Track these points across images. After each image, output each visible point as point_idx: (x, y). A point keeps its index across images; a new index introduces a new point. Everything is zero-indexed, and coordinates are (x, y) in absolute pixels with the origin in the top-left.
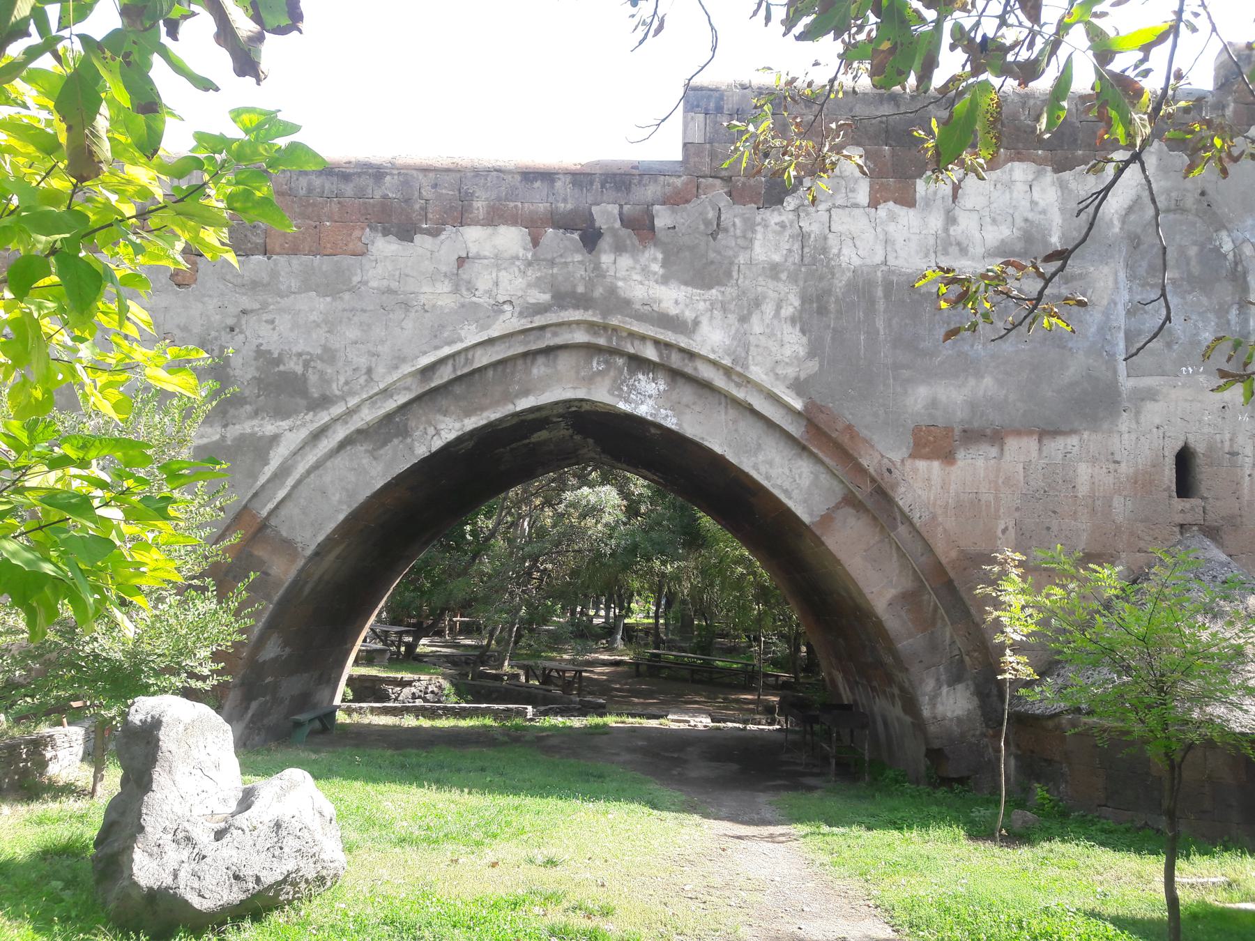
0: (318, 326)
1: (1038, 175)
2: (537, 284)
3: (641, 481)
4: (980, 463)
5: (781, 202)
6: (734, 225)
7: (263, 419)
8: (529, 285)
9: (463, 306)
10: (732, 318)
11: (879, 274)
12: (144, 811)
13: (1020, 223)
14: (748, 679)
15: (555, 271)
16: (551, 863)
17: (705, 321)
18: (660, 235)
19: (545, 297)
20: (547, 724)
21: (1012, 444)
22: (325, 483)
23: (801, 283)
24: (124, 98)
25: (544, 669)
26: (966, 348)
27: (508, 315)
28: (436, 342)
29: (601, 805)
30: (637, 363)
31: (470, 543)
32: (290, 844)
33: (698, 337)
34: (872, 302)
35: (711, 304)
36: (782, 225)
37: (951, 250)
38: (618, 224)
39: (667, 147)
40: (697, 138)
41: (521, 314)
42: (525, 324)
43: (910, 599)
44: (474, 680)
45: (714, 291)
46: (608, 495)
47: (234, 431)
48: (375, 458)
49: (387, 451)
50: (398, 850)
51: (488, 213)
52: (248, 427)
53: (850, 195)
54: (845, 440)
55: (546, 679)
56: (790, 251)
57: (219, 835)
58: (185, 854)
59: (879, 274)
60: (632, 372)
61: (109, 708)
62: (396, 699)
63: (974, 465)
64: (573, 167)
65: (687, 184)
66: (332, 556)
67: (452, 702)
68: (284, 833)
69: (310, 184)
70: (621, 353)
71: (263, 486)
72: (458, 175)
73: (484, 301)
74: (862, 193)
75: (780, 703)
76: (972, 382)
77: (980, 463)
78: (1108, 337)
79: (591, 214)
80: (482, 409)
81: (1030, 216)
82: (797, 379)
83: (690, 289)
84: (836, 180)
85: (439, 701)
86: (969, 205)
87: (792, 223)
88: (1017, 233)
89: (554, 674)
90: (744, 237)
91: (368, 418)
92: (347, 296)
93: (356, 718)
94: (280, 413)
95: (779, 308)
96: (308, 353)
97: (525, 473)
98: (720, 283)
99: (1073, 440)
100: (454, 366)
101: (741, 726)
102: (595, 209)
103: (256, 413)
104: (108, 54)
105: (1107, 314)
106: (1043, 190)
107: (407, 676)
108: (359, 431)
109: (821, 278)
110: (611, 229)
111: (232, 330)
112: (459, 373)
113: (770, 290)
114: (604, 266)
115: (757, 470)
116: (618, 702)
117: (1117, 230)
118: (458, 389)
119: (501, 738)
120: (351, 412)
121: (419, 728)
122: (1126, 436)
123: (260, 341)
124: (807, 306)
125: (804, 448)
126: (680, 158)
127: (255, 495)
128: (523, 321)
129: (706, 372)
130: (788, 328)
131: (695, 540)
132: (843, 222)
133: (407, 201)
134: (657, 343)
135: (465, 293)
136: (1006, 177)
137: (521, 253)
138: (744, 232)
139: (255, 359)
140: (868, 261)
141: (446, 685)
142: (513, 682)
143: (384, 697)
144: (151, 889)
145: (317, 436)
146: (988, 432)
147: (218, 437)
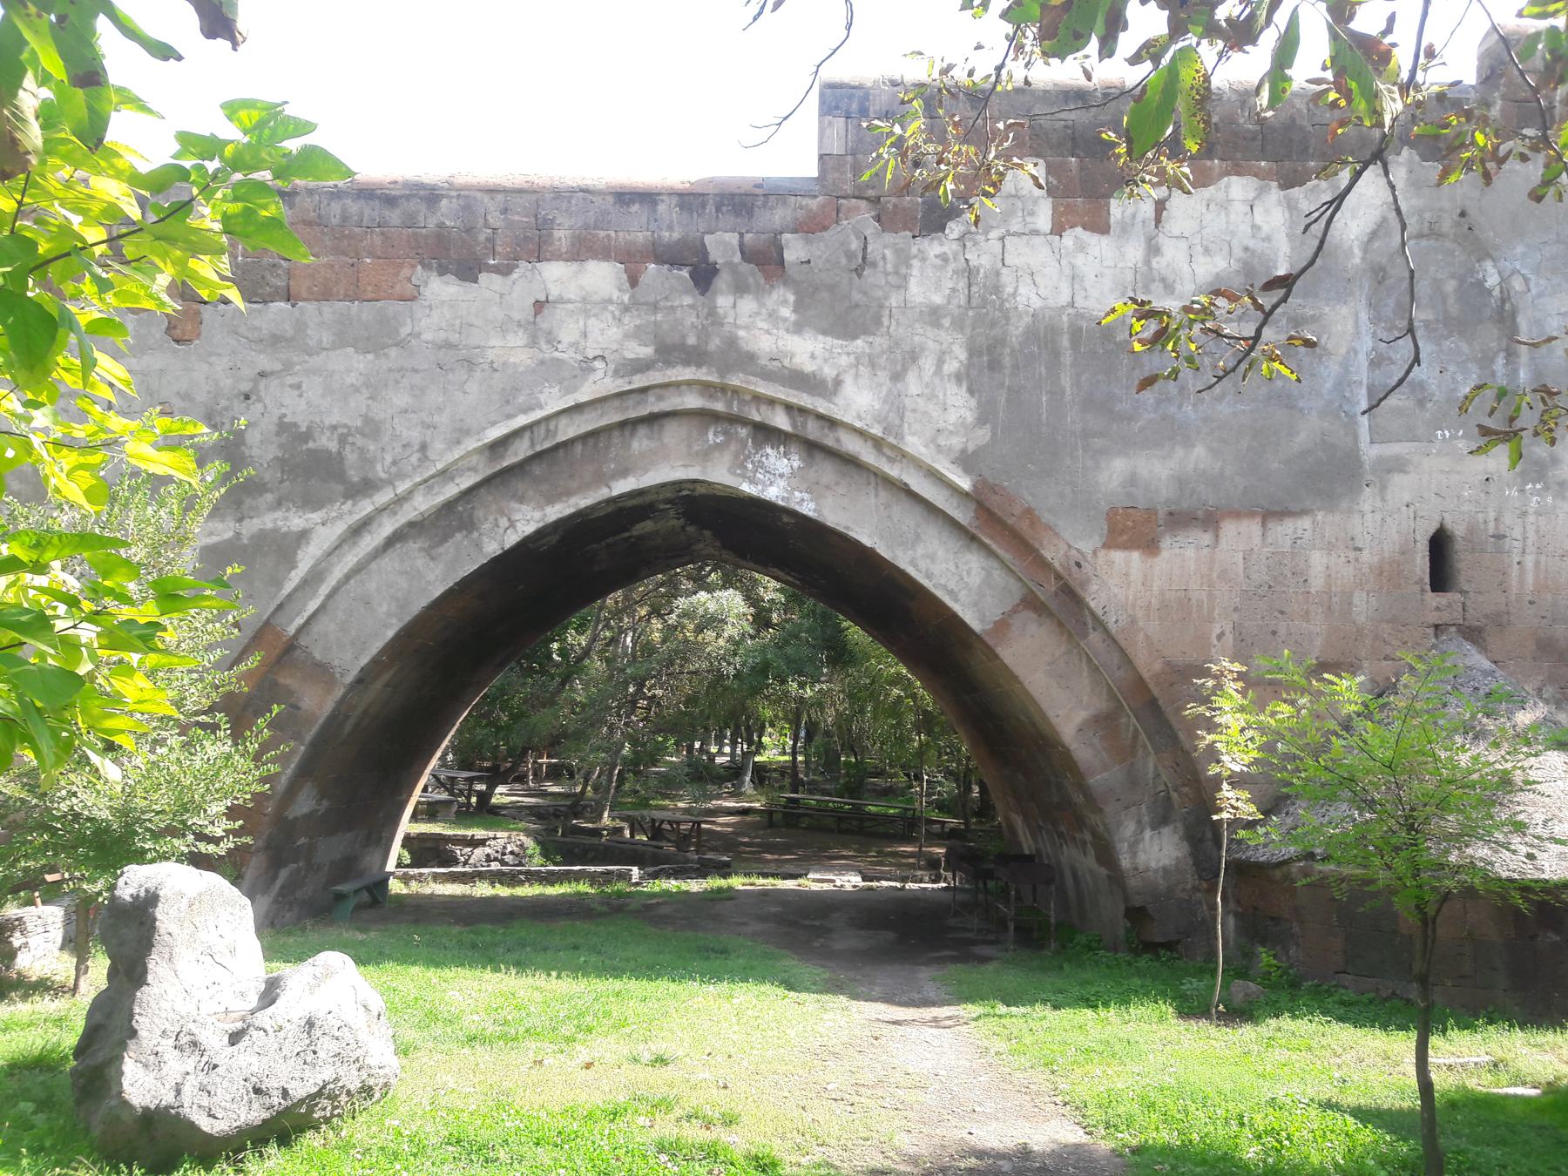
0: (357, 390)
1: (1262, 191)
2: (637, 334)
3: (773, 584)
4: (1190, 553)
5: (942, 228)
6: (884, 258)
7: (288, 510)
8: (627, 336)
9: (542, 362)
10: (883, 376)
11: (1065, 318)
12: (137, 1010)
13: (1238, 252)
14: (908, 828)
15: (659, 317)
16: (661, 1061)
17: (848, 380)
18: (792, 271)
19: (646, 351)
20: (657, 889)
21: (1229, 529)
22: (368, 591)
23: (968, 331)
24: (53, 63)
25: (653, 821)
26: (1173, 409)
27: (600, 374)
28: (509, 409)
29: (724, 987)
30: (765, 434)
31: (557, 665)
32: (326, 1047)
33: (840, 400)
34: (1056, 354)
35: (857, 359)
36: (944, 258)
37: (1153, 287)
38: (737, 258)
40: (836, 148)
41: (616, 373)
42: (623, 385)
43: (1105, 723)
44: (565, 836)
45: (859, 342)
46: (731, 602)
47: (251, 527)
48: (433, 559)
49: (448, 549)
50: (467, 1050)
51: (573, 245)
52: (268, 521)
53: (1028, 219)
54: (1024, 527)
55: (656, 833)
56: (953, 290)
57: (235, 1038)
58: (190, 1063)
59: (1065, 318)
60: (758, 446)
61: (93, 881)
62: (465, 863)
63: (1183, 555)
64: (681, 186)
65: (823, 206)
66: (379, 685)
67: (537, 864)
68: (319, 1033)
69: (344, 210)
70: (744, 422)
71: (289, 596)
72: (534, 197)
73: (569, 356)
74: (1043, 217)
75: (947, 855)
76: (1179, 452)
77: (1190, 553)
78: (1348, 394)
79: (703, 245)
80: (569, 493)
81: (1251, 244)
82: (963, 451)
83: (829, 339)
84: (1011, 200)
85: (520, 864)
86: (1176, 232)
87: (955, 255)
88: (1235, 266)
89: (666, 826)
90: (897, 273)
91: (423, 508)
92: (393, 352)
93: (415, 887)
94: (311, 502)
95: (940, 362)
96: (345, 426)
97: (626, 575)
98: (866, 332)
99: (1305, 523)
100: (532, 440)
101: (898, 885)
102: (708, 239)
103: (279, 504)
104: (32, 9)
105: (1346, 366)
106: (1267, 211)
107: (479, 833)
108: (411, 525)
109: (993, 324)
110: (729, 264)
111: (247, 397)
112: (538, 449)
113: (929, 339)
114: (721, 311)
115: (916, 566)
116: (747, 860)
117: (1357, 261)
118: (537, 470)
119: (596, 906)
120: (400, 500)
121: (495, 898)
122: (1369, 516)
123: (283, 411)
124: (975, 360)
125: (973, 538)
126: (816, 174)
127: (280, 607)
128: (620, 381)
129: (851, 445)
130: (952, 388)
131: (840, 655)
132: (1021, 254)
133: (469, 230)
134: (789, 408)
135: (544, 346)
136: (1221, 195)
137: (615, 295)
138: (896, 266)
139: (278, 434)
140: (1051, 303)
141: (529, 843)
142: (615, 838)
143: (453, 861)
144: (146, 1109)
145: (357, 530)
146: (1200, 514)
147: (229, 535)
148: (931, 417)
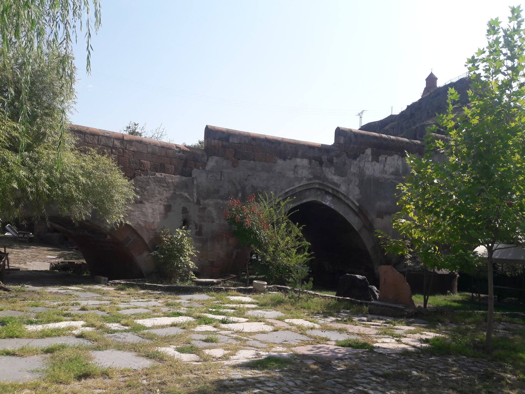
1: (399, 158)
39: (329, 140)
74: (370, 159)
102: (322, 157)
129: (341, 196)
134: (332, 189)
148: (352, 192)
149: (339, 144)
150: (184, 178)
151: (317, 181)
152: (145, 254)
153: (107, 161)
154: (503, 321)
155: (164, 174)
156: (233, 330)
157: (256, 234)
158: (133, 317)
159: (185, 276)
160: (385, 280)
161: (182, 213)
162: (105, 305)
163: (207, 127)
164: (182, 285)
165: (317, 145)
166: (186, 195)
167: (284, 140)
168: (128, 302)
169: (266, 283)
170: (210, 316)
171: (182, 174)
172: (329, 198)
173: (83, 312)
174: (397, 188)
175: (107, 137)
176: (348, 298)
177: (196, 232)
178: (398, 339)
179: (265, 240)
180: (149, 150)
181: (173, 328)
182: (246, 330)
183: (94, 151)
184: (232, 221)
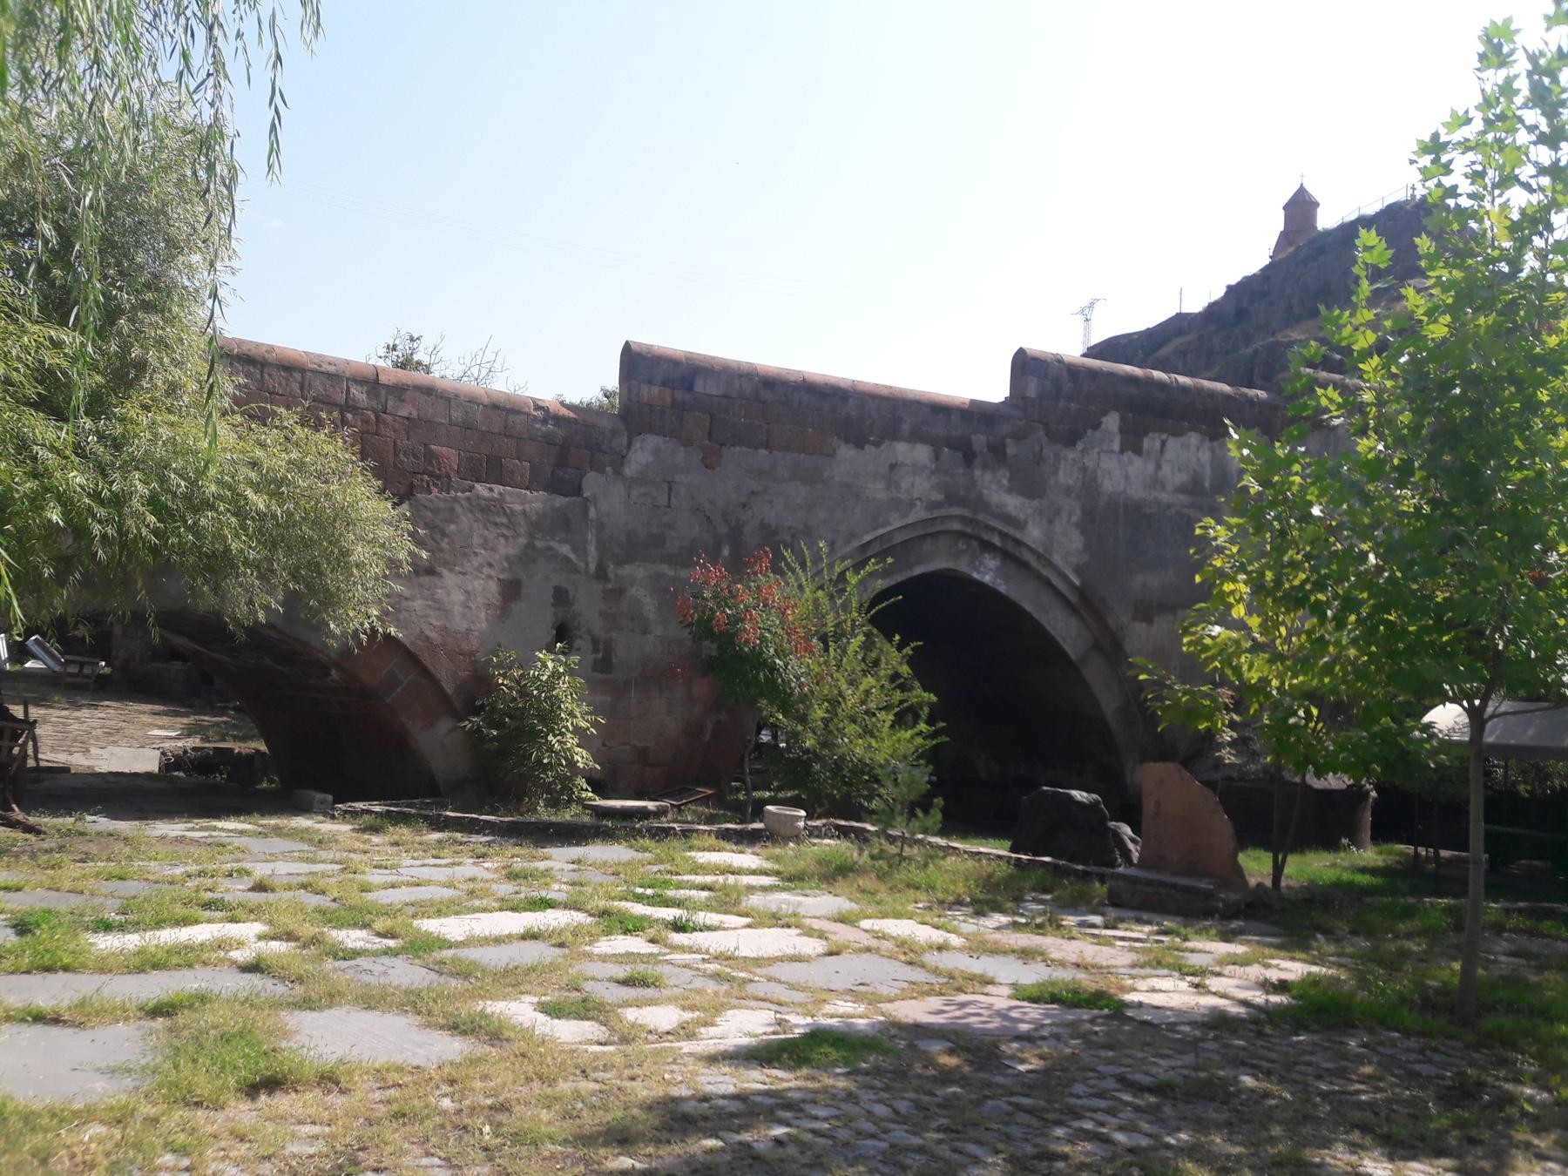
19: (941, 497)
39: (994, 388)
73: (903, 496)
74: (1116, 446)
95: (1070, 516)
129: (1027, 556)
134: (1002, 534)
148: (1061, 543)
149: (1024, 398)
150: (560, 501)
151: (956, 511)
152: (444, 725)
153: (329, 448)
154: (1510, 931)
155: (498, 488)
156: (707, 952)
157: (773, 669)
158: (410, 911)
159: (561, 792)
160: (1158, 804)
161: (554, 605)
162: (324, 875)
163: (627, 345)
164: (553, 819)
165: (957, 402)
166: (565, 549)
167: (860, 388)
168: (393, 867)
169: (803, 813)
170: (638, 909)
171: (554, 487)
172: (992, 562)
173: (259, 897)
174: (1198, 531)
175: (329, 375)
176: (1047, 859)
177: (596, 661)
178: (1196, 980)
179: (801, 686)
180: (454, 414)
181: (530, 945)
182: (745, 952)
183: (289, 418)
184: (704, 628)
